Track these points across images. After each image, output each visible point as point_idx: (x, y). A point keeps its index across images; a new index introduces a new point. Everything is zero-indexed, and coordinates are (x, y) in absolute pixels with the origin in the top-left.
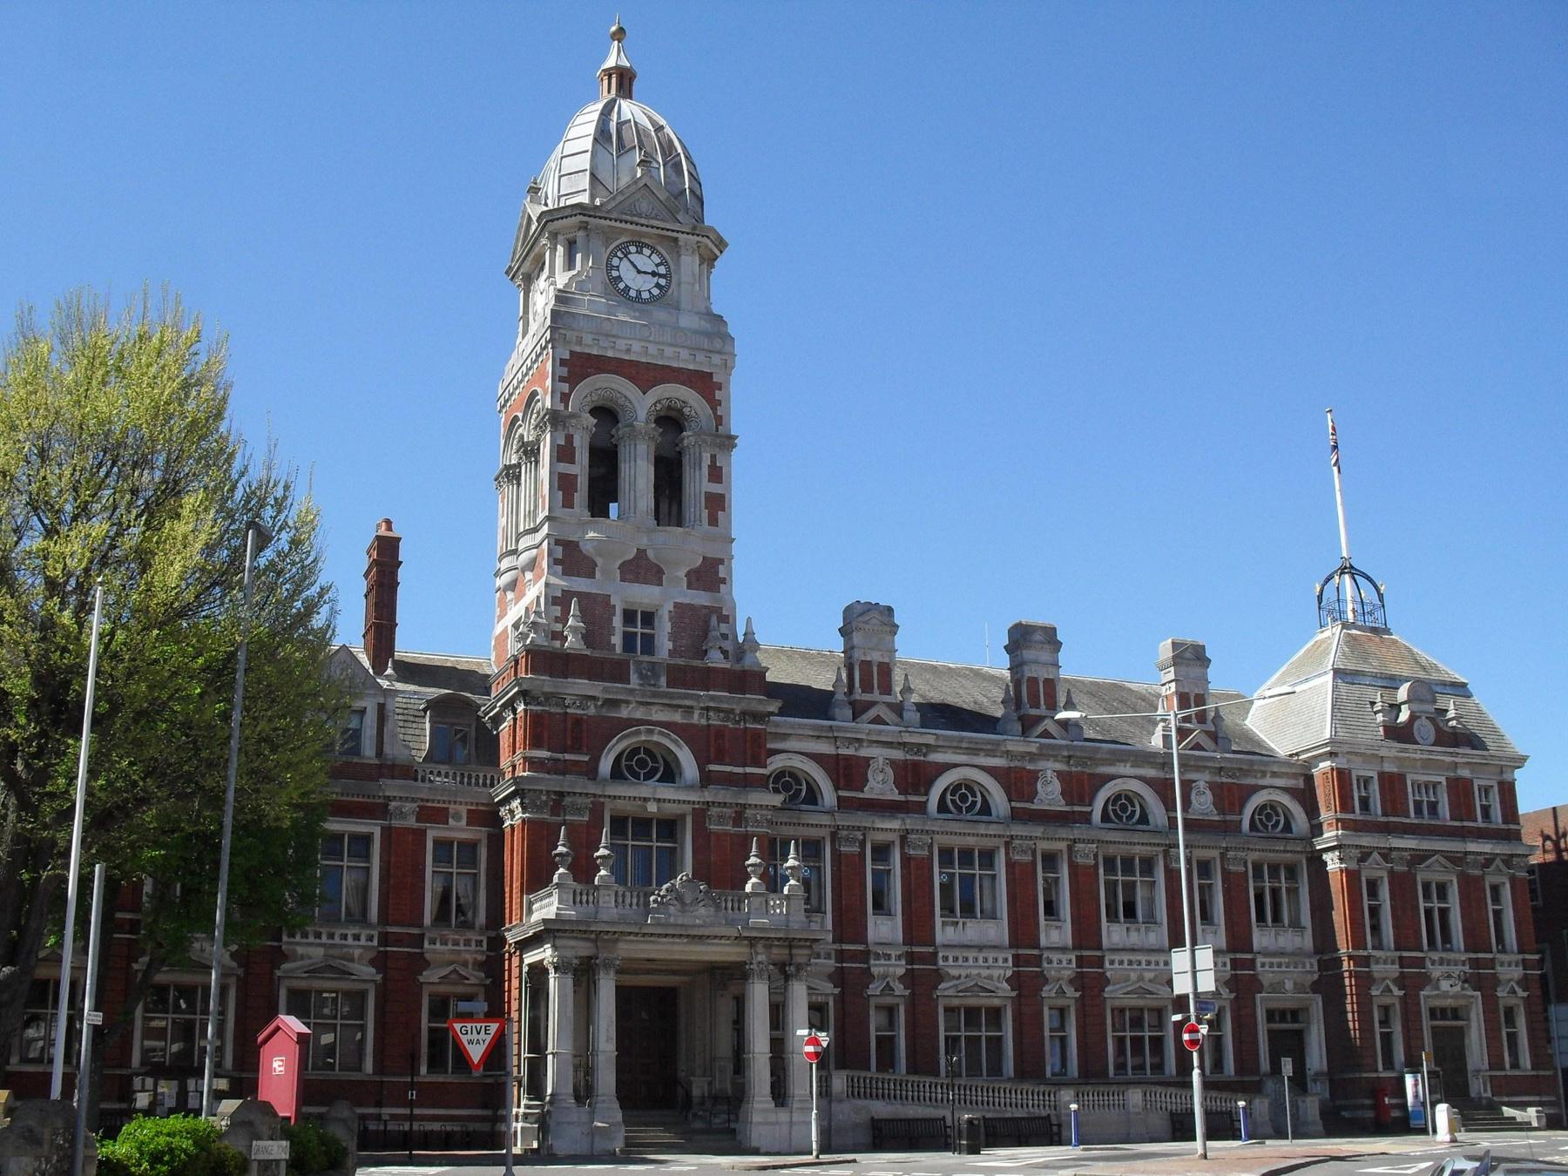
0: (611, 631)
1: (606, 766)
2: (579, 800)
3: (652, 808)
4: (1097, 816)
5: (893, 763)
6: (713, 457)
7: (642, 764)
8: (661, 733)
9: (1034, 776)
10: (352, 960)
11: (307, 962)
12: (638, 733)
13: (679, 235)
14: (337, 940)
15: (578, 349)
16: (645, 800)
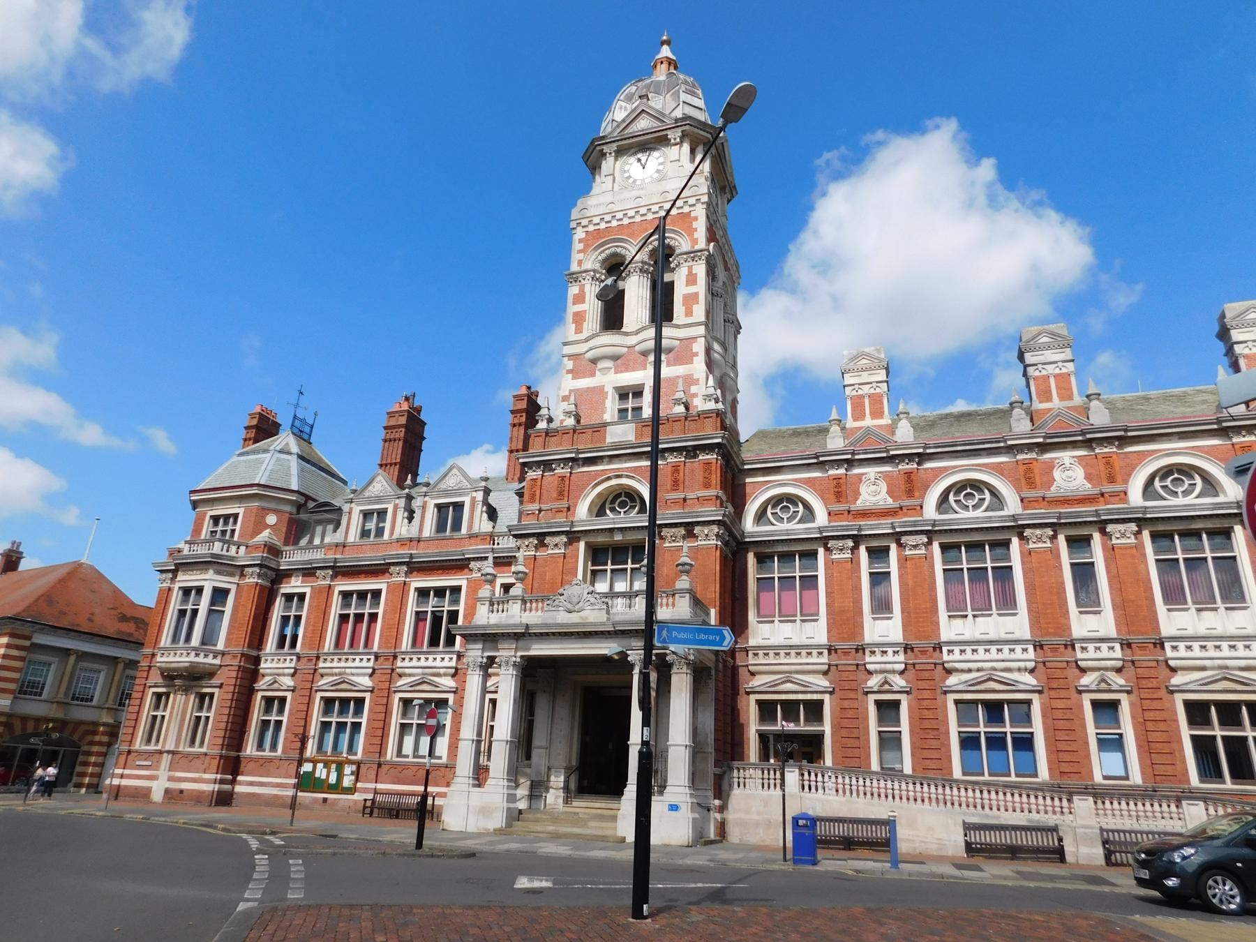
0: (603, 410)
1: (582, 510)
2: (557, 539)
3: (618, 537)
4: (1135, 496)
5: (886, 476)
6: (690, 268)
7: (623, 505)
8: (628, 477)
9: (1050, 466)
10: (438, 675)
11: (413, 679)
12: (609, 479)
13: (669, 132)
14: (430, 663)
15: (591, 228)
16: (611, 530)
